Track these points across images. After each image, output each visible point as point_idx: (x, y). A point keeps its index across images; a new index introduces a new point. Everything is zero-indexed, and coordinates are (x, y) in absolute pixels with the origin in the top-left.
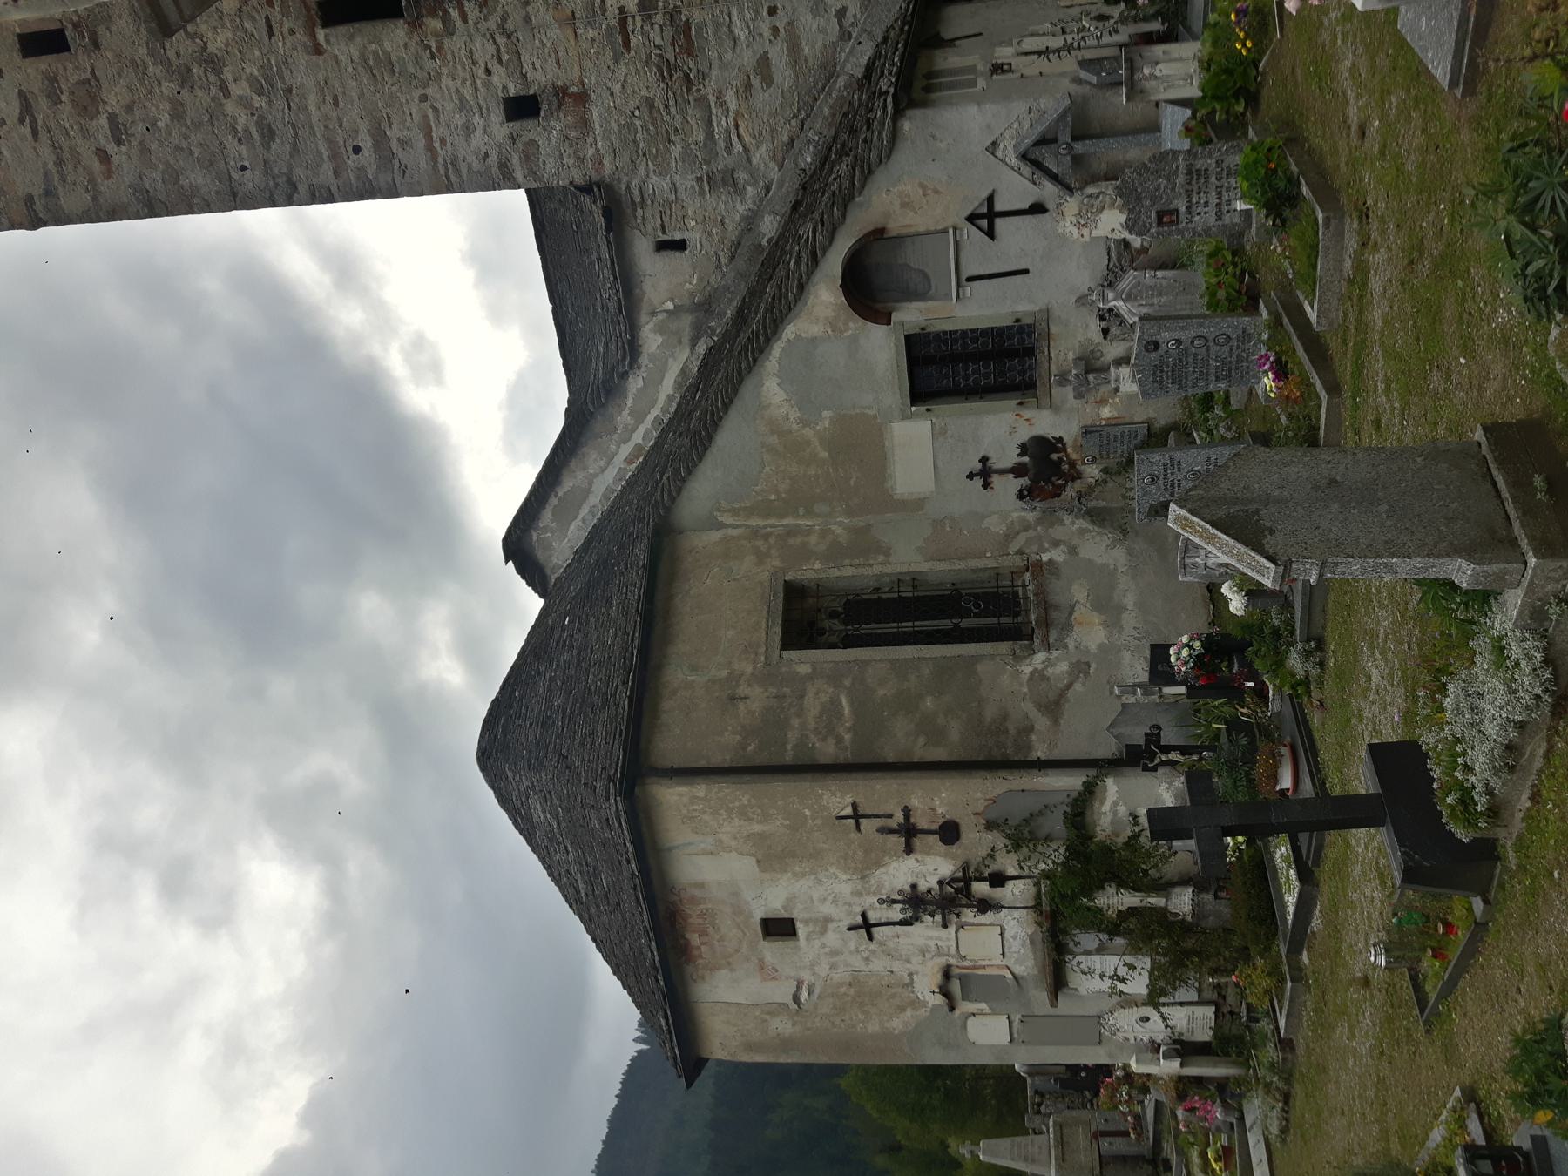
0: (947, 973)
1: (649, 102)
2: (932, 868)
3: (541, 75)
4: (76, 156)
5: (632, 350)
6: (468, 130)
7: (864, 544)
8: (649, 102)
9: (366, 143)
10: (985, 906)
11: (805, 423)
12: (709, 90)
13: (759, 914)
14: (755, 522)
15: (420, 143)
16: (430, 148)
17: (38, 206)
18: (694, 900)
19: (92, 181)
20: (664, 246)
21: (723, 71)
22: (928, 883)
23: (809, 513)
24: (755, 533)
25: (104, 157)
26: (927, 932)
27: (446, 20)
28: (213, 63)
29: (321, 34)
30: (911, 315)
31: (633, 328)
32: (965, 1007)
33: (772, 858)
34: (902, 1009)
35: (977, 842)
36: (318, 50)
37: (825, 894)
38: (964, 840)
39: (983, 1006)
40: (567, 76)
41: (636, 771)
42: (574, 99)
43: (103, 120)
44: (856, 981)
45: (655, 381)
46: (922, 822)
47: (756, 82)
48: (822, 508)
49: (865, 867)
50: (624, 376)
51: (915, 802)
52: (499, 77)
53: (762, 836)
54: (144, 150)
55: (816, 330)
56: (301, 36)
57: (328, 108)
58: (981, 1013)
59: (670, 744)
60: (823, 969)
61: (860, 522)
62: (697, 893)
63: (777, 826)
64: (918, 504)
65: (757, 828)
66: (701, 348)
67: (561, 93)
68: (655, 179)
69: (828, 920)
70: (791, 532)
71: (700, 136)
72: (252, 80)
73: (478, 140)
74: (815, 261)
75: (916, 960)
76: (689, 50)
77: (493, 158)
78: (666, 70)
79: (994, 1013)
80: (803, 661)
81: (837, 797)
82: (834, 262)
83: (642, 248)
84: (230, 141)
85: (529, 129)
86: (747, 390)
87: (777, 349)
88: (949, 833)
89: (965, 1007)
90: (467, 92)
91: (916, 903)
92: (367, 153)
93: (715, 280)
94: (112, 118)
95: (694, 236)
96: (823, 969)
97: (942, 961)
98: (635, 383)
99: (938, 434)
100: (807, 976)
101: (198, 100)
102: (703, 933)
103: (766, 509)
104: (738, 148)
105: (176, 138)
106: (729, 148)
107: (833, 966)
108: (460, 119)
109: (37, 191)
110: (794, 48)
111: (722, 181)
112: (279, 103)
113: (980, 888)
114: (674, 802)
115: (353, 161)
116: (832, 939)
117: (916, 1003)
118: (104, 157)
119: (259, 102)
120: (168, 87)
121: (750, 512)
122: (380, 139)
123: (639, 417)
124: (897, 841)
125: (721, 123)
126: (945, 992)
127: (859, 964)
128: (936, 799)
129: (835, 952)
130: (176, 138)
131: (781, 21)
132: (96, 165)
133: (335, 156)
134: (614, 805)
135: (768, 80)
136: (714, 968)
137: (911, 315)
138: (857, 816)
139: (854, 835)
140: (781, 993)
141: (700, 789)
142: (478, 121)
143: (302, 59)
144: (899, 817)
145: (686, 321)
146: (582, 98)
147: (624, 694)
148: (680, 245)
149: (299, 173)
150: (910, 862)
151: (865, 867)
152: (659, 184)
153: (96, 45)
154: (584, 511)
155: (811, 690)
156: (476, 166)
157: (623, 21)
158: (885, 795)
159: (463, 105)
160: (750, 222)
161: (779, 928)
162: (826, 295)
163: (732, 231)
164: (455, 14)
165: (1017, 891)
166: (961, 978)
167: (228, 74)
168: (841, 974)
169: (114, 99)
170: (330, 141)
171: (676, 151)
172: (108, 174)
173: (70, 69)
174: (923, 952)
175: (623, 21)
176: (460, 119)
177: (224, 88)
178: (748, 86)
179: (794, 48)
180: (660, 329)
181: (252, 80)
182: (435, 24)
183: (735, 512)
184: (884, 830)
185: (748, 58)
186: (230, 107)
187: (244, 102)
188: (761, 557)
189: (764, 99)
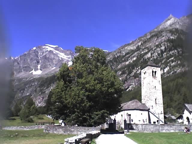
2: (145, 120)
67: (153, 108)
169: (153, 89)
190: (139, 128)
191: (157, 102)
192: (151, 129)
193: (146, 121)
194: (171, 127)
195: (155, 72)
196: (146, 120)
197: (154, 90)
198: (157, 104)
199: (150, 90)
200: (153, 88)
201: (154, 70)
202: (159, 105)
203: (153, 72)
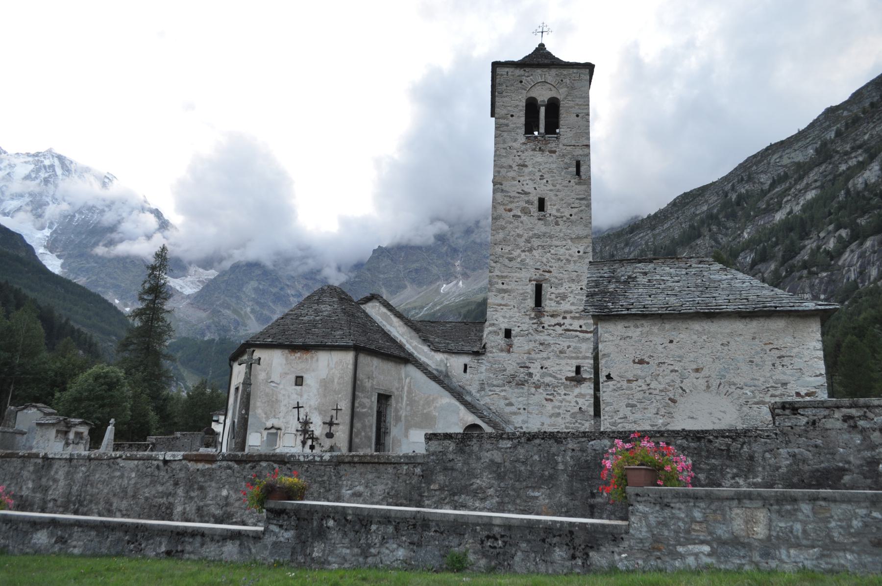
0: (279, 429)
1: (505, 370)
2: (318, 428)
3: (516, 341)
4: (511, 202)
5: (437, 350)
6: (504, 317)
7: (398, 419)
8: (505, 370)
9: (505, 287)
10: (304, 443)
11: (435, 408)
12: (506, 388)
13: (305, 376)
14: (406, 388)
15: (503, 302)
16: (501, 305)
17: (499, 186)
18: (312, 358)
19: (504, 204)
20: (466, 366)
21: (512, 393)
22: (312, 427)
23: (407, 405)
24: (403, 388)
25: (510, 210)
26: (295, 425)
27: (533, 318)
28: (530, 250)
29: (534, 283)
31: (443, 352)
32: (265, 433)
33: (325, 384)
34: (266, 414)
35: (327, 443)
36: (530, 281)
39: (265, 438)
40: (514, 348)
41: (358, 349)
42: (509, 349)
43: (519, 214)
44: (277, 401)
45: (426, 356)
46: (334, 428)
47: (507, 402)
48: (409, 408)
49: (321, 411)
50: (429, 346)
51: (341, 427)
52: (518, 330)
53: (333, 381)
54: (511, 223)
55: (461, 415)
56: (534, 277)
57: (515, 279)
58: (262, 438)
59: (364, 359)
60: (283, 392)
61: (403, 418)
62: (315, 359)
63: (336, 386)
64: (406, 436)
65: (336, 380)
66: (435, 372)
67: (511, 346)
68: (485, 368)
69: (301, 396)
70: (402, 398)
71: (495, 383)
72: (525, 260)
73: (501, 319)
74: (480, 417)
75: (284, 420)
76: (517, 384)
77: (496, 322)
78: (513, 376)
79: (262, 442)
80: (375, 398)
81: (345, 405)
82: (479, 422)
83: (466, 359)
84: (510, 248)
85: (502, 335)
86: (447, 393)
87: (457, 403)
88: (330, 435)
89: (265, 433)
90: (514, 319)
92: (500, 286)
93: (454, 380)
94: (519, 217)
95: (468, 376)
96: (283, 392)
97: (283, 428)
98: (426, 349)
100: (281, 387)
101: (521, 242)
102: (299, 358)
103: (410, 392)
104: (490, 393)
105: (513, 233)
106: (490, 391)
107: (284, 395)
108: (508, 316)
109: (503, 187)
110: (515, 414)
111: (482, 388)
112: (518, 265)
113: (309, 442)
114: (348, 357)
115: (500, 282)
116: (294, 396)
117: (268, 418)
118: (510, 210)
119: (519, 260)
120: (526, 236)
121: (409, 388)
122: (505, 291)
123: (415, 348)
124: (328, 420)
125: (497, 389)
127: (283, 403)
129: (289, 397)
130: (513, 233)
131: (522, 411)
132: (508, 207)
133: (502, 277)
134: (351, 343)
135: (507, 405)
136: (287, 359)
138: (337, 409)
139: (330, 408)
140: (275, 377)
142: (506, 320)
143: (528, 276)
144: (336, 422)
145: (443, 369)
146: (509, 351)
147: (373, 347)
148: (465, 371)
149: (499, 265)
150: (320, 423)
152: (483, 368)
153: (539, 219)
154: (384, 323)
155: (368, 400)
156: (494, 317)
157: (527, 367)
158: (344, 419)
159: (511, 317)
160: (469, 393)
161: (299, 381)
163: (467, 387)
164: (535, 321)
166: (276, 434)
167: (527, 253)
168: (280, 397)
169: (524, 218)
170: (506, 277)
171: (491, 375)
172: (505, 210)
173: (534, 209)
174: (287, 423)
175: (527, 367)
176: (508, 316)
177: (524, 251)
178: (506, 399)
179: (515, 414)
180: (442, 361)
181: (525, 260)
182: (533, 316)
183: (410, 383)
184: (332, 417)
185: (513, 400)
186: (519, 251)
187: (519, 256)
188: (397, 389)
189: (502, 403)
191: (549, 305)
193: (330, 435)
195: (553, 107)
196: (331, 424)
197: (531, 223)
198: (547, 320)
199: (501, 222)
200: (525, 211)
201: (542, 95)
202: (559, 320)
203: (532, 106)
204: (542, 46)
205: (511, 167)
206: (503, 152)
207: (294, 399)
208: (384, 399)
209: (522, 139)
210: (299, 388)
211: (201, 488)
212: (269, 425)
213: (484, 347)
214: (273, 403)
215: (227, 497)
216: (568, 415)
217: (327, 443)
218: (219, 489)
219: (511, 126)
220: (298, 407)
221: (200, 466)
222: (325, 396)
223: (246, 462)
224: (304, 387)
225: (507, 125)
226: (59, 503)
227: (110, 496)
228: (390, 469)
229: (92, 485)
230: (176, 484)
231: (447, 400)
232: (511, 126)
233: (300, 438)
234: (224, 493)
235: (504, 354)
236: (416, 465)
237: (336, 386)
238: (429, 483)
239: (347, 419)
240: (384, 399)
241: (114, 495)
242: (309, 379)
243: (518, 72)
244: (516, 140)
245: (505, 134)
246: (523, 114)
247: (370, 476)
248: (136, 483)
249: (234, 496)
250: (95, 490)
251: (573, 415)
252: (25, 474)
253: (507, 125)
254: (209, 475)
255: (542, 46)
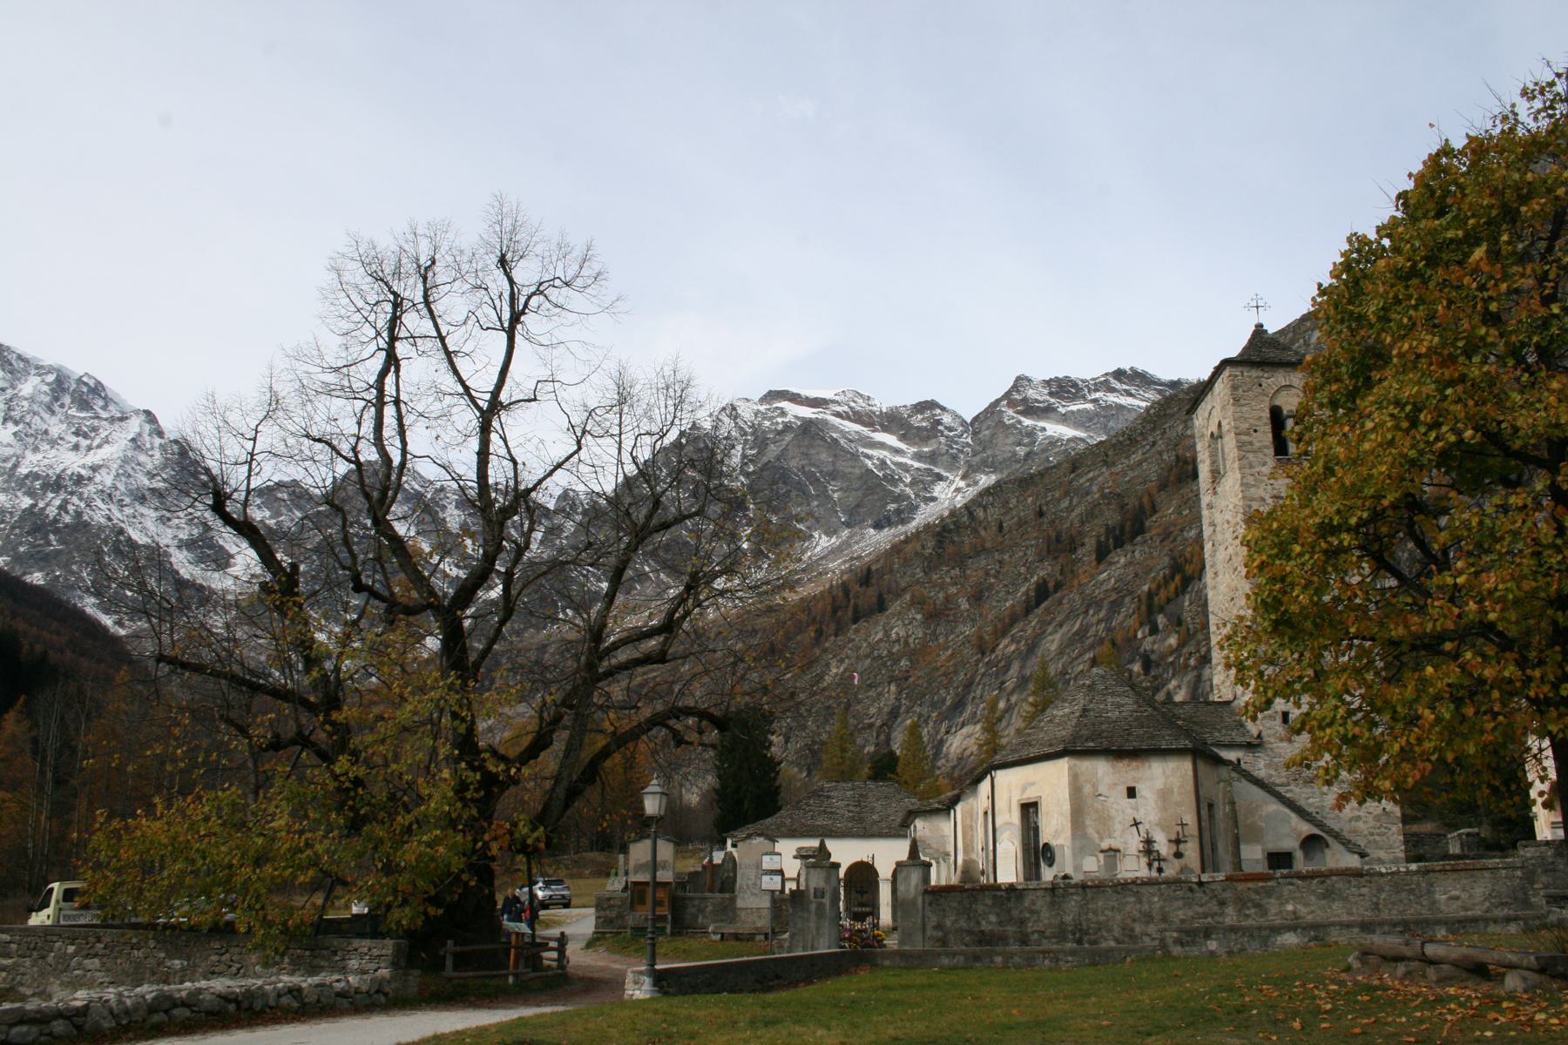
2: (1163, 846)
10: (1150, 865)
13: (1138, 787)
22: (1156, 847)
26: (1134, 843)
30: (1299, 855)
32: (1101, 856)
33: (1164, 795)
37: (1148, 808)
38: (1176, 861)
44: (1110, 818)
46: (1182, 846)
49: (1162, 826)
51: (1189, 845)
63: (1176, 797)
81: (1190, 818)
82: (1317, 831)
86: (1273, 799)
87: (1287, 811)
88: (1178, 855)
91: (1149, 842)
99: (1257, 861)
113: (1156, 864)
116: (1129, 811)
117: (1101, 838)
124: (1174, 837)
126: (1111, 849)
127: (1119, 819)
128: (1191, 850)
137: (1299, 855)
140: (1102, 789)
141: (1190, 773)
151: (1162, 826)
161: (1131, 792)
162: (1307, 829)
165: (1154, 874)
168: (1113, 813)
190: (1030, 927)
192: (1138, 928)
193: (1178, 855)
194: (1328, 895)
196: (1178, 842)
204: (1259, 326)
205: (1263, 499)
206: (1251, 480)
207: (1130, 814)
208: (1211, 806)
209: (1271, 462)
210: (1132, 801)
211: (1258, 906)
212: (1105, 845)
213: (1259, 736)
214: (1105, 820)
215: (1294, 912)
216: (1370, 818)
217: (1177, 863)
218: (1281, 904)
219: (1257, 444)
220: (1136, 824)
221: (1250, 885)
222: (1164, 809)
223: (1312, 877)
224: (1138, 799)
225: (1251, 443)
226: (1048, 933)
227: (1129, 921)
228: (1486, 874)
229: (1095, 913)
230: (1222, 903)
231: (1273, 807)
232: (1257, 444)
233: (1144, 860)
234: (1290, 907)
235: (1285, 744)
236: (1515, 868)
237: (1176, 797)
238: (1532, 883)
239: (1196, 833)
240: (1211, 806)
241: (1134, 920)
242: (1142, 789)
243: (1255, 373)
244: (1265, 464)
245: (1251, 456)
246: (1268, 428)
247: (1464, 881)
248: (1162, 908)
249: (1302, 910)
250: (1102, 918)
251: (1377, 818)
252: (980, 908)
253: (1251, 443)
254: (1269, 893)
255: (1259, 326)
